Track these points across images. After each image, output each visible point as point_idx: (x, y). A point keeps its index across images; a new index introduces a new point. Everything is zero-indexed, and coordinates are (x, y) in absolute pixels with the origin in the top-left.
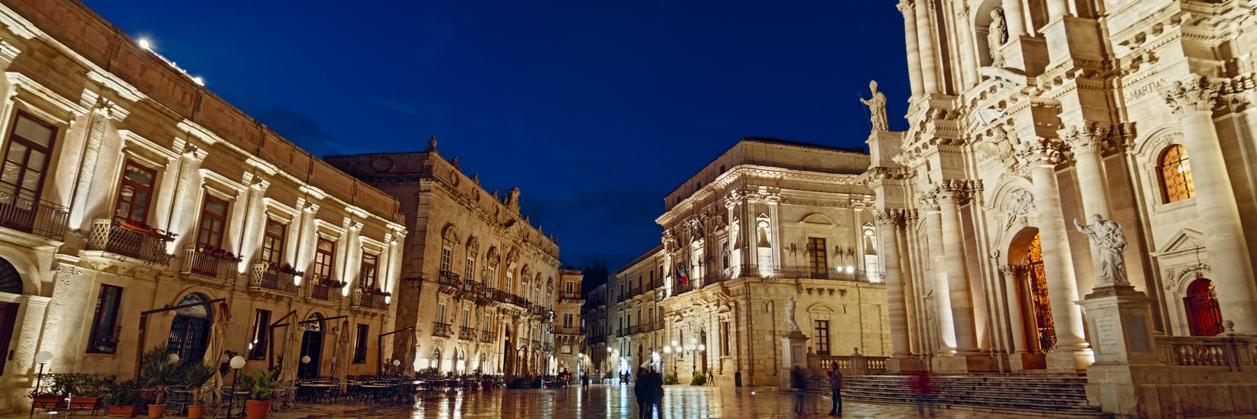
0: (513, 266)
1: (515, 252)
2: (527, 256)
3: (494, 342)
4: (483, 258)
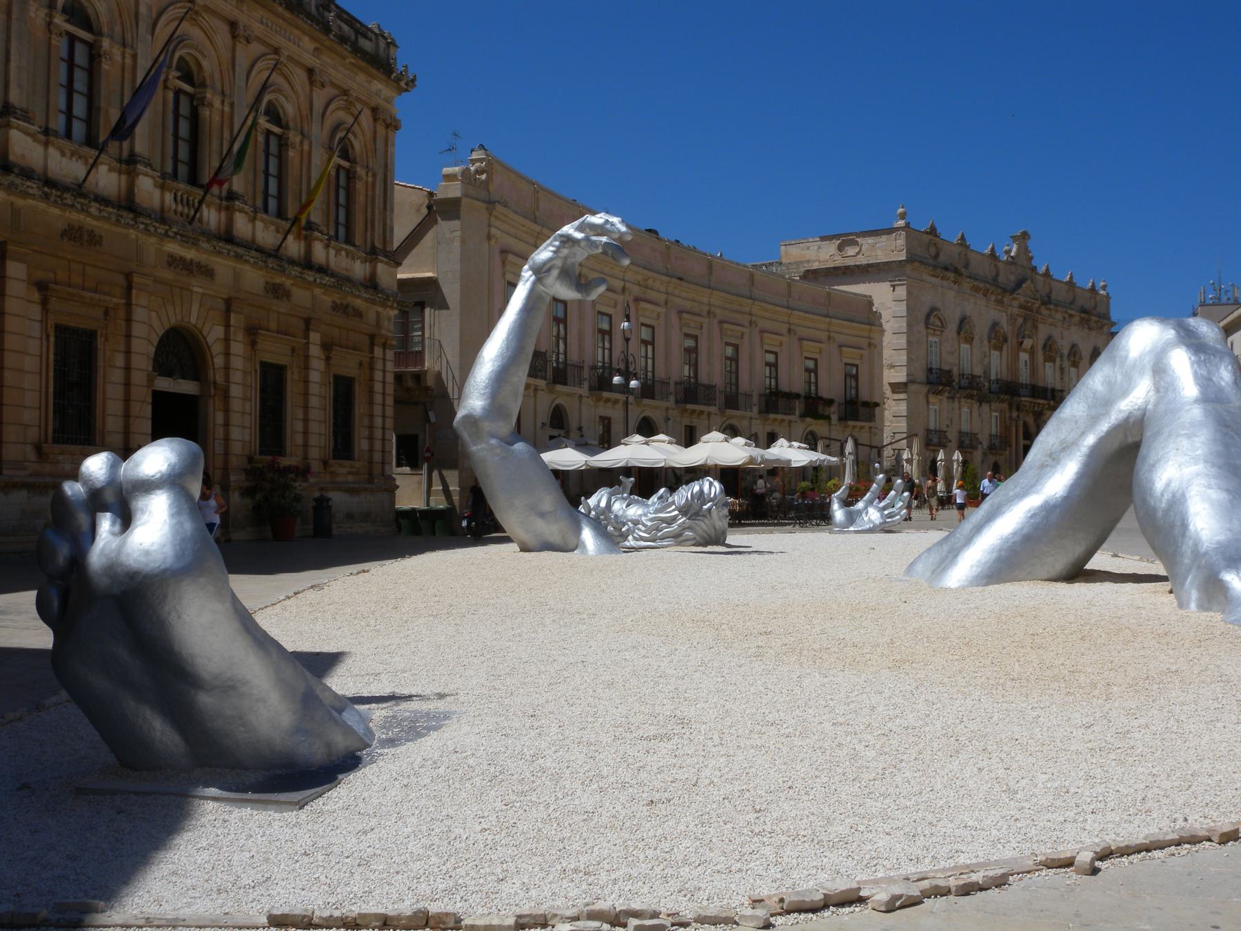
0: (1028, 343)
1: (1029, 324)
2: (1051, 325)
3: (1008, 448)
4: (982, 341)
